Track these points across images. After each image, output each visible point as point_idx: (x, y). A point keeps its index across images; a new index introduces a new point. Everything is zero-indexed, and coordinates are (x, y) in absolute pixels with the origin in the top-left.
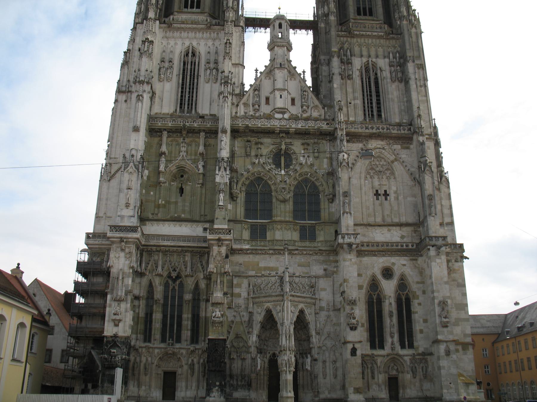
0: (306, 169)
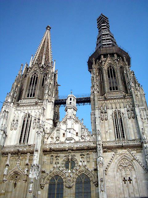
0: (83, 168)
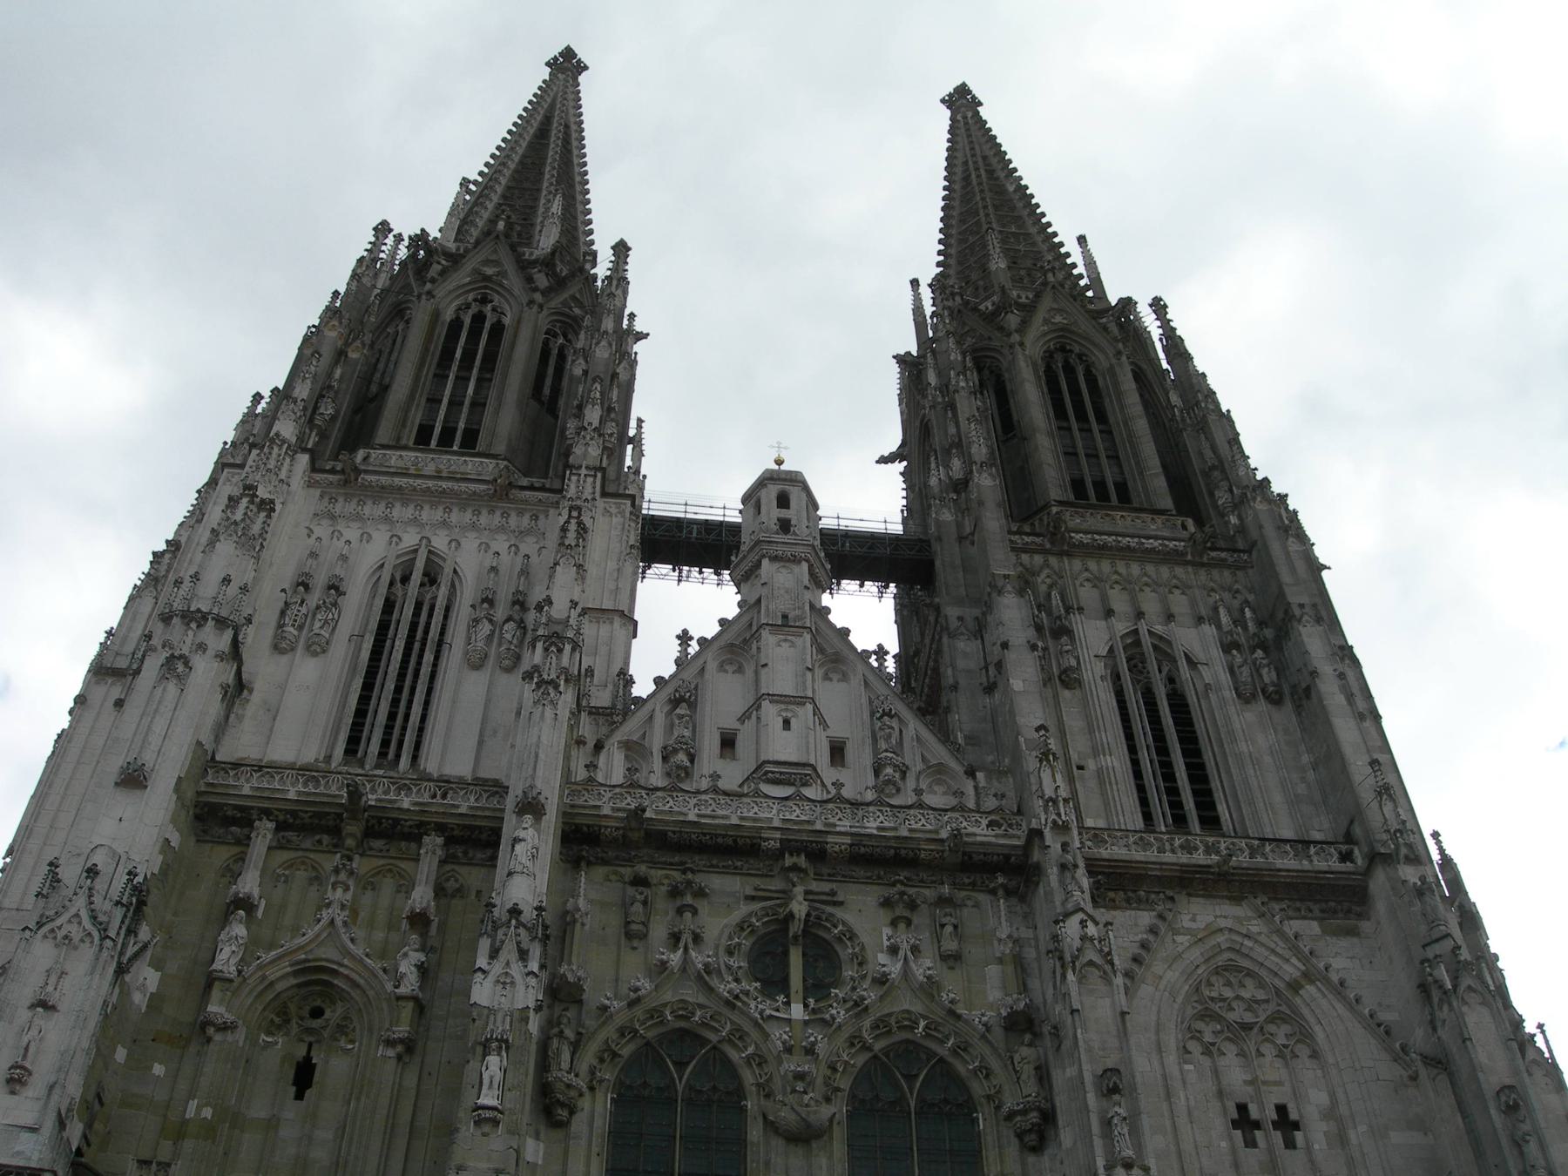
0: (908, 1003)
